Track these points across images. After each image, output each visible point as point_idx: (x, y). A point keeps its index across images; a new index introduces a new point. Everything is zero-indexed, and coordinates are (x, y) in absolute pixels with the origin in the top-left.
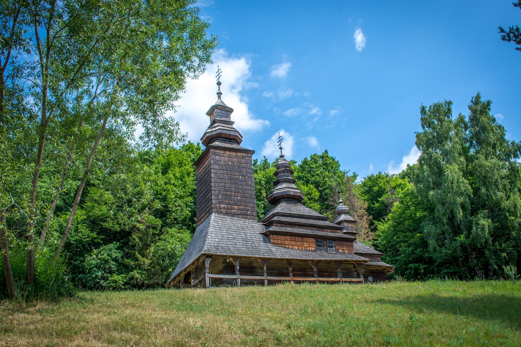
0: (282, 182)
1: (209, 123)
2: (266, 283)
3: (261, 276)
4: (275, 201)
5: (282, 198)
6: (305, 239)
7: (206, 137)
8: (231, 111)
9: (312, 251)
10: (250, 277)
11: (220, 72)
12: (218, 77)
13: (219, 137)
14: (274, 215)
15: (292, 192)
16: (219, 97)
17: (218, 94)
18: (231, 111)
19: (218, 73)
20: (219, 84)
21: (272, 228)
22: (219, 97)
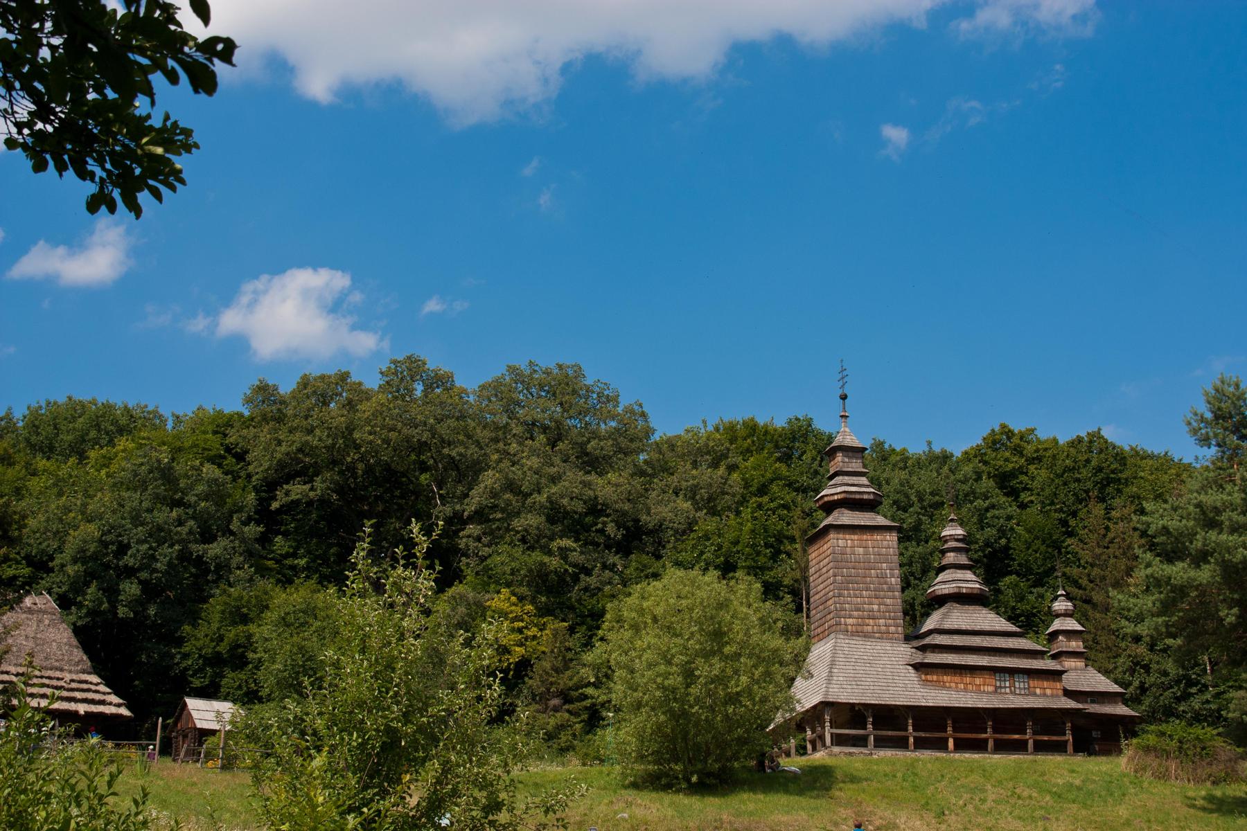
2: (911, 740)
4: (940, 601)
9: (988, 693)
10: (890, 733)
11: (845, 373)
12: (841, 383)
15: (965, 587)
20: (844, 397)
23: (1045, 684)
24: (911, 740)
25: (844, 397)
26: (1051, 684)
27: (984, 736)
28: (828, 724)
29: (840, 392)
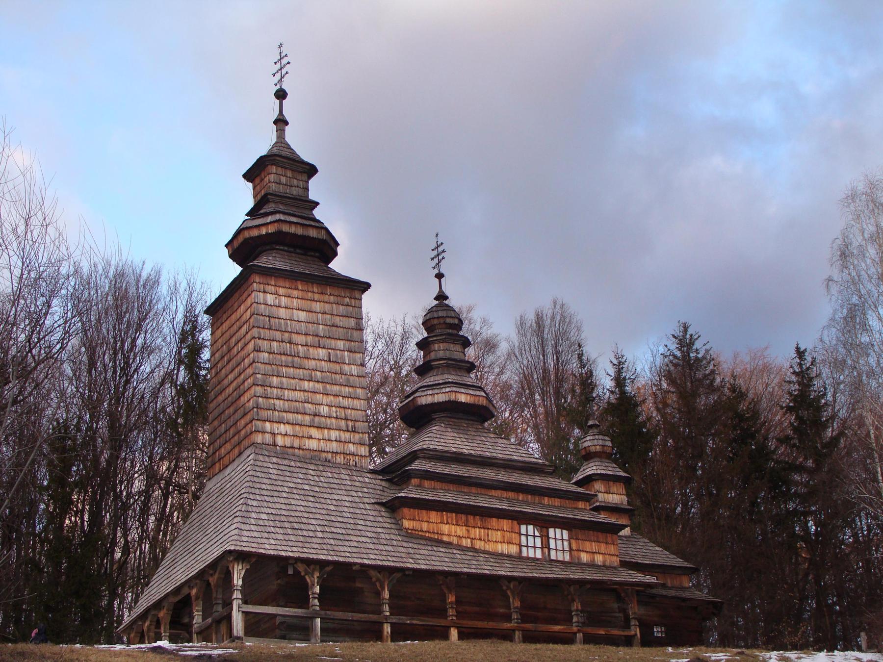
0: (438, 367)
1: (250, 204)
2: (387, 629)
3: (373, 613)
5: (435, 412)
6: (494, 522)
7: (241, 239)
8: (312, 170)
11: (284, 61)
12: (278, 76)
13: (278, 241)
14: (414, 456)
16: (281, 133)
17: (275, 122)
18: (312, 170)
19: (278, 66)
20: (281, 95)
21: (411, 492)
22: (281, 133)
23: (594, 546)
24: (387, 629)
25: (281, 95)
26: (603, 548)
27: (507, 625)
28: (237, 595)
29: (278, 87)
